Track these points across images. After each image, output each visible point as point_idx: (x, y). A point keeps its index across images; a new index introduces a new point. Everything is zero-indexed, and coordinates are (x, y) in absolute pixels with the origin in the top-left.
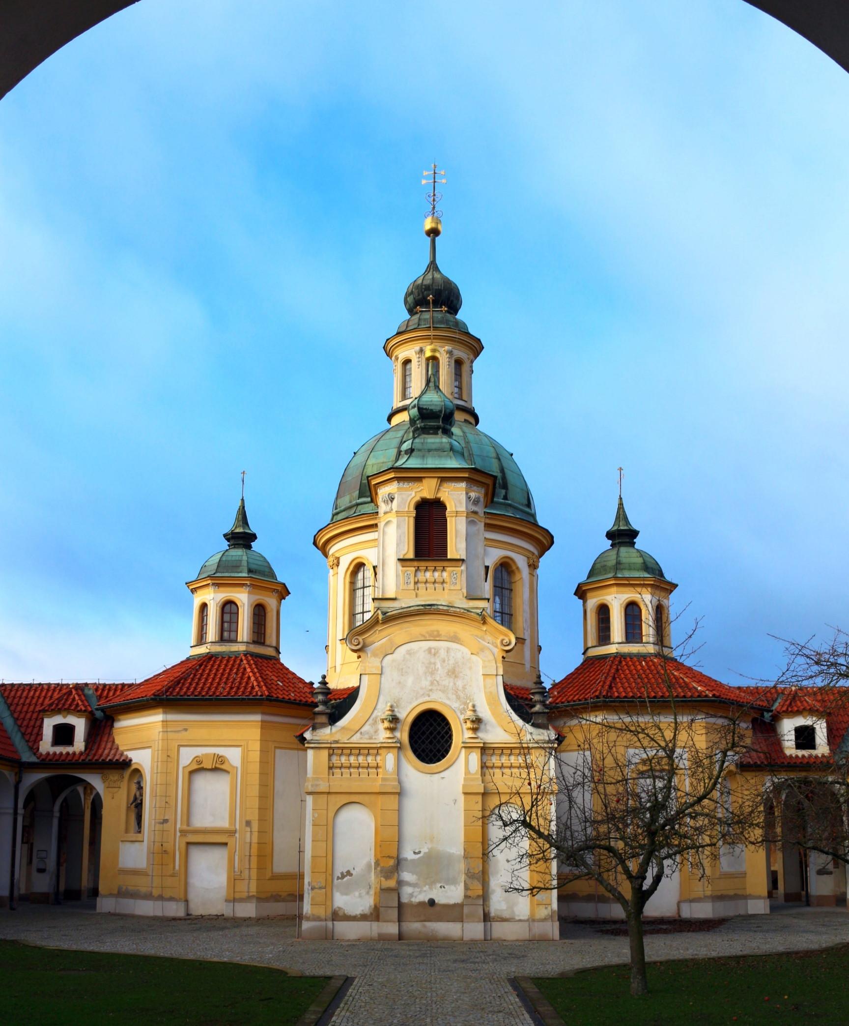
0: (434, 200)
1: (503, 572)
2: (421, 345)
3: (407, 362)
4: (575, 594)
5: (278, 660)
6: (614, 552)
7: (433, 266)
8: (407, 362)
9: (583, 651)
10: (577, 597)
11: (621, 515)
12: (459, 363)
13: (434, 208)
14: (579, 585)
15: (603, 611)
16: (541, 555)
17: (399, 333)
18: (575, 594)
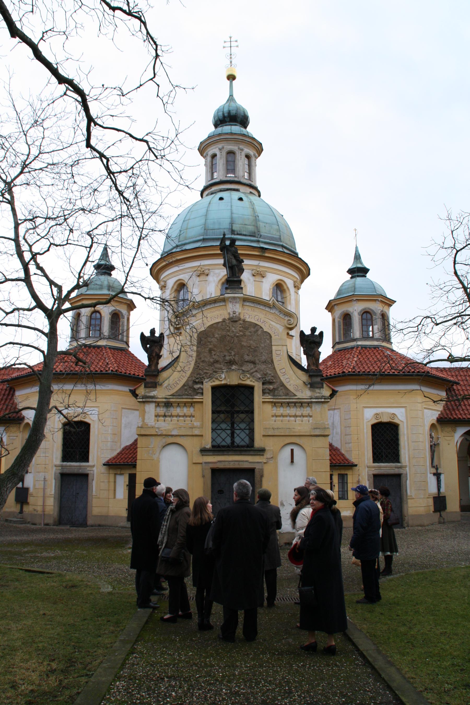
0: (231, 58)
1: (278, 291)
2: (223, 145)
3: (214, 156)
4: (326, 309)
5: (128, 350)
6: (354, 279)
7: (231, 98)
8: (214, 156)
9: (332, 346)
10: (327, 311)
11: (357, 257)
12: (248, 157)
13: (231, 62)
14: (330, 301)
15: (347, 318)
16: (302, 281)
17: (208, 137)
18: (326, 309)
